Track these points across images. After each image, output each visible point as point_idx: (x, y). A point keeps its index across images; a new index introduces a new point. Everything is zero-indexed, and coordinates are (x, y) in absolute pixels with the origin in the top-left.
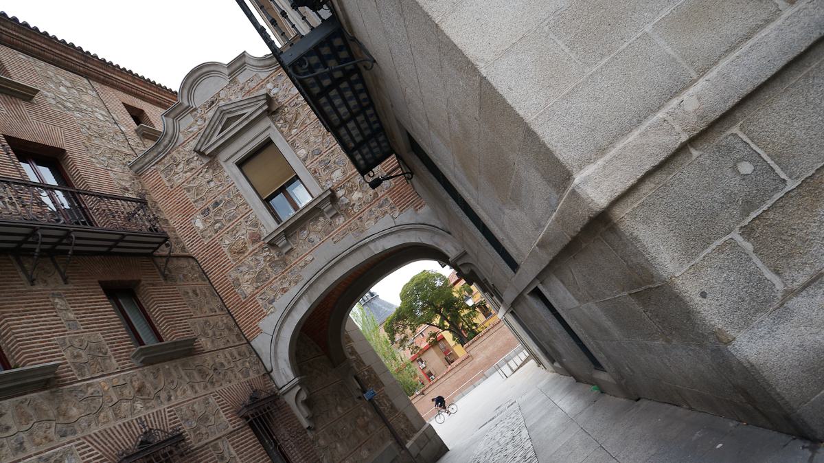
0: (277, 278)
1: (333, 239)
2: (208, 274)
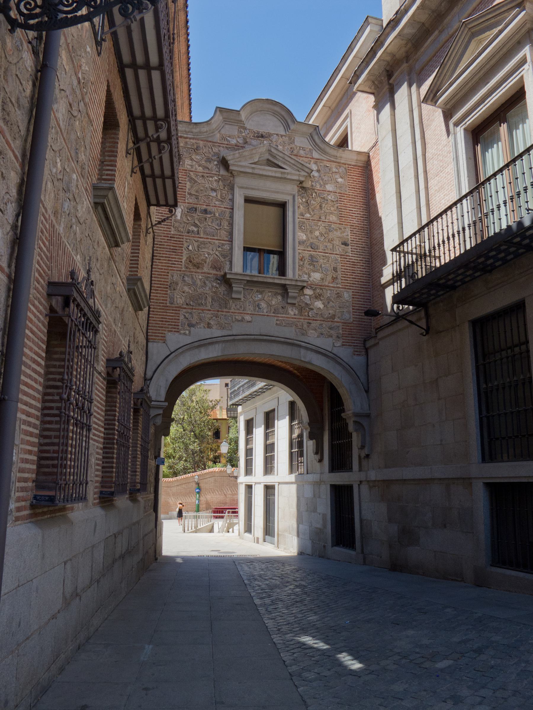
0: (210, 310)
1: (277, 320)
2: (155, 258)
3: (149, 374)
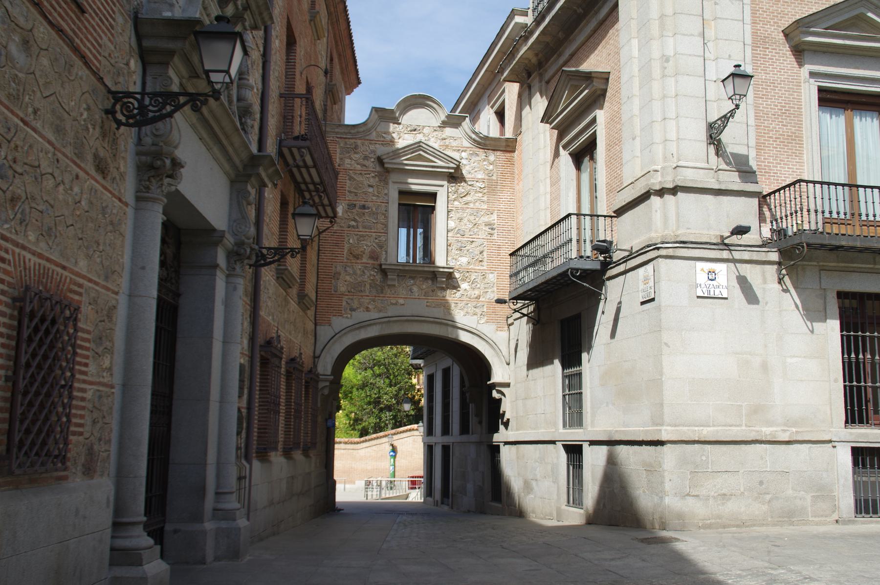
3: (318, 353)
